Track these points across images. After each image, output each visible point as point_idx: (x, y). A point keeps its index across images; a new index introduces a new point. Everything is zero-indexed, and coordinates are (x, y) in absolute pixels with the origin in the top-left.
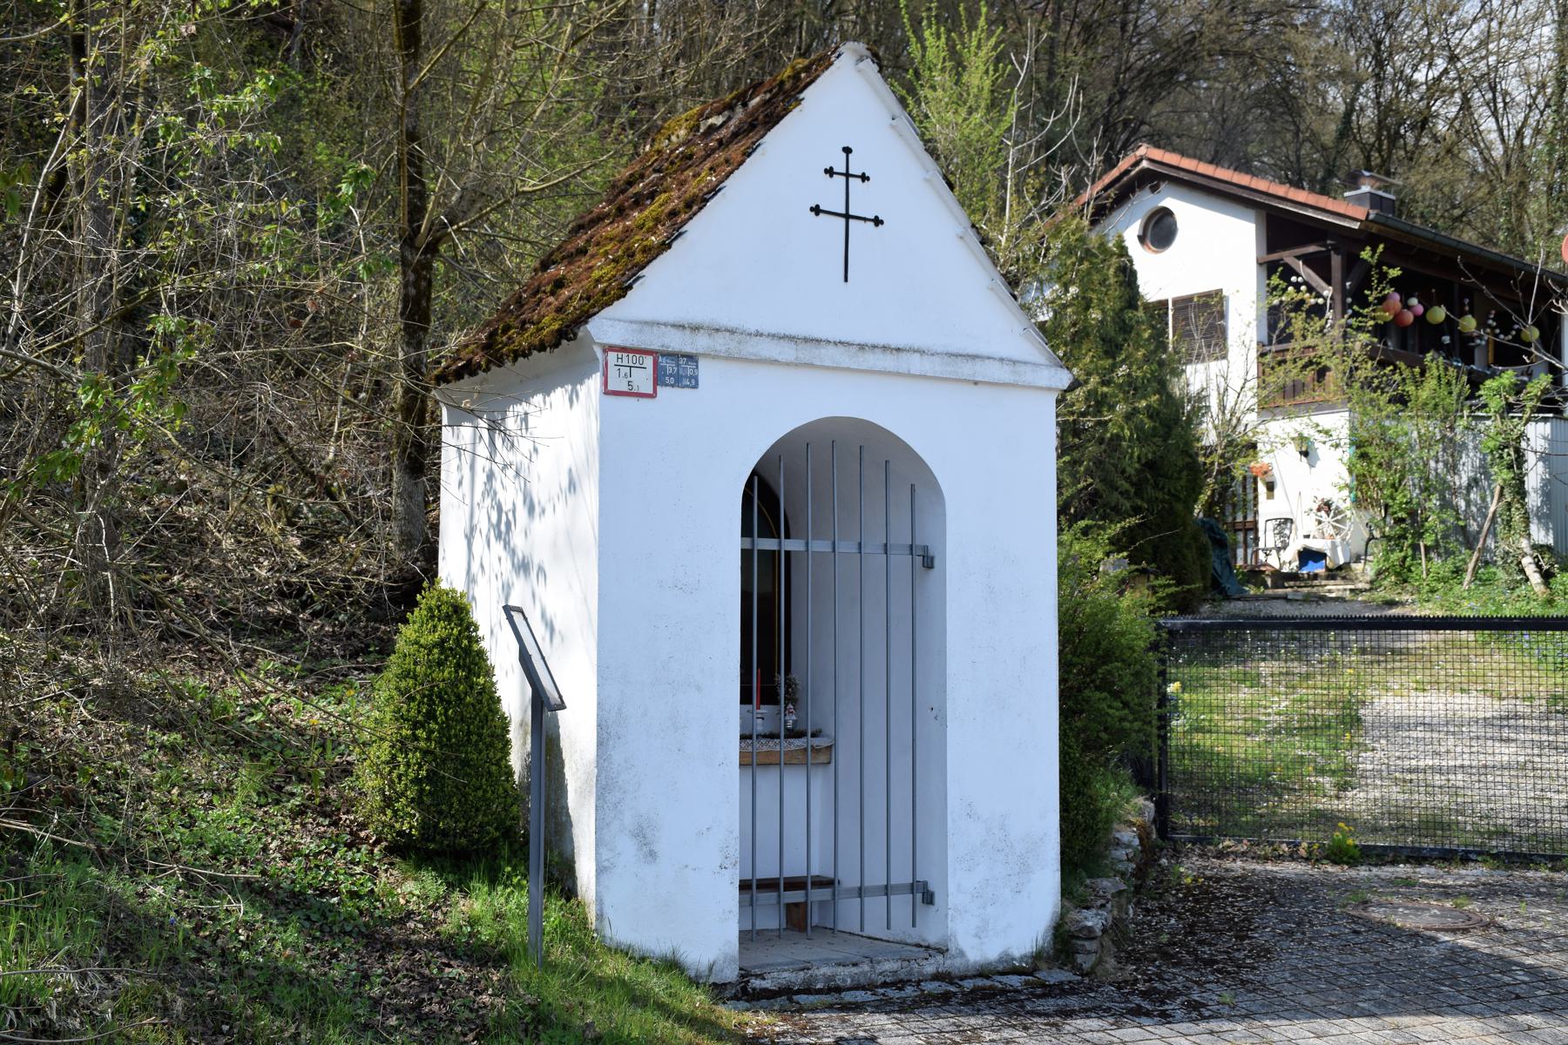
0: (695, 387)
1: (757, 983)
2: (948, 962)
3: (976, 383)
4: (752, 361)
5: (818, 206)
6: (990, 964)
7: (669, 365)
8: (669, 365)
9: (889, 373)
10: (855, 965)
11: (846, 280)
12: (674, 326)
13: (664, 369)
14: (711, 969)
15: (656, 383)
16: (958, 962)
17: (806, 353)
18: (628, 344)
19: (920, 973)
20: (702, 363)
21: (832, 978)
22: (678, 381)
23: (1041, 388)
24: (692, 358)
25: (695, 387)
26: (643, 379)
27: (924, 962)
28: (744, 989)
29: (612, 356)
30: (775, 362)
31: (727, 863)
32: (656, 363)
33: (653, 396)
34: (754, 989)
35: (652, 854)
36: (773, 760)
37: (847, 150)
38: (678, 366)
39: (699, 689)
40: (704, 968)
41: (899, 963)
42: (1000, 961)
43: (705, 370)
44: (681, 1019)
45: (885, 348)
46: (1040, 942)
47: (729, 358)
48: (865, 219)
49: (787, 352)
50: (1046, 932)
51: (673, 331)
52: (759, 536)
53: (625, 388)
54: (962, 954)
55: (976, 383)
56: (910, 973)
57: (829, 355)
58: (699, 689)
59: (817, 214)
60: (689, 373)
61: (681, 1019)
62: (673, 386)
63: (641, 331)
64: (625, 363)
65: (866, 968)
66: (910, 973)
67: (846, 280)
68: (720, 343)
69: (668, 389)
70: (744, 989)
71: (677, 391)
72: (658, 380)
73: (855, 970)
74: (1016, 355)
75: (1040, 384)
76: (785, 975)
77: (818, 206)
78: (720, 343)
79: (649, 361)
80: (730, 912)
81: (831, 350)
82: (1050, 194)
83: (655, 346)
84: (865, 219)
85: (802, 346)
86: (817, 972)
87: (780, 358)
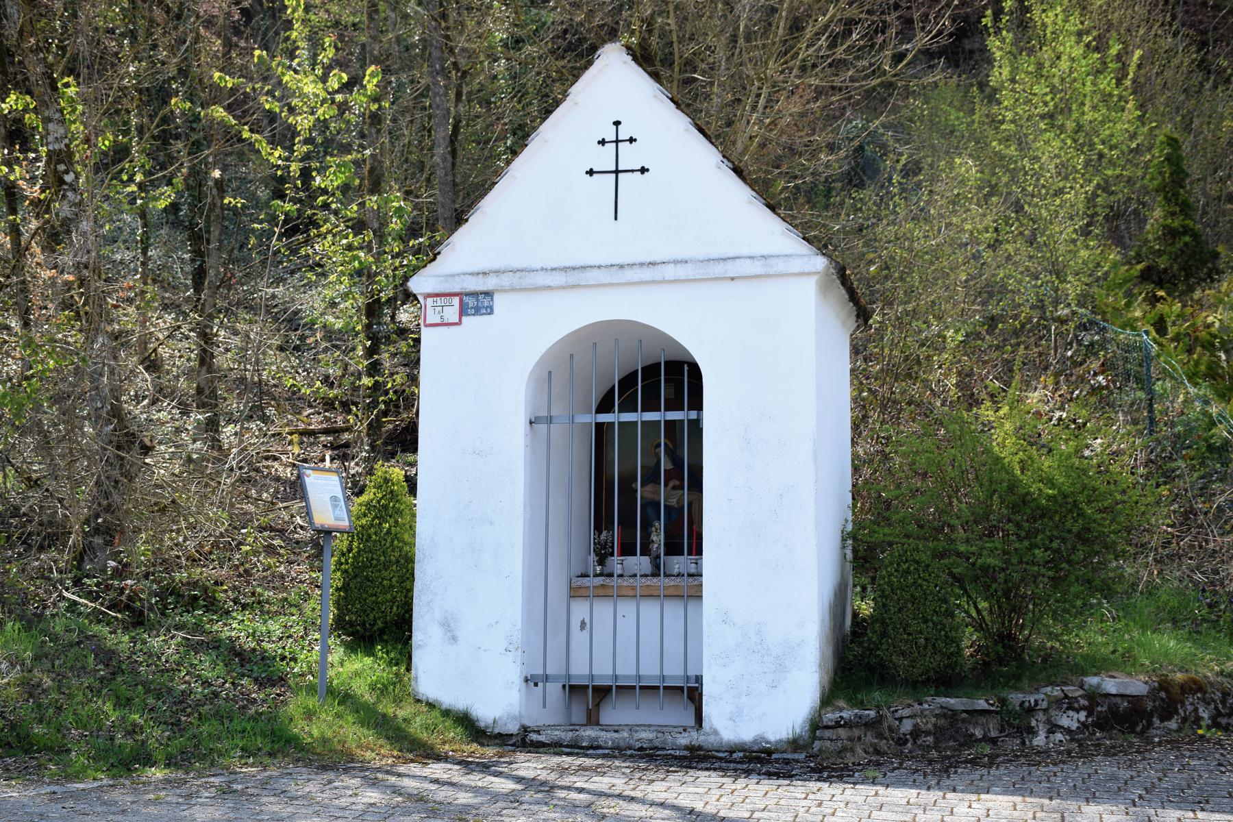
0: (491, 313)
1: (534, 737)
2: (702, 738)
3: (733, 279)
4: (530, 290)
5: (591, 169)
6: (745, 743)
7: (471, 302)
8: (471, 302)
9: (695, 280)
10: (616, 731)
11: (616, 219)
12: (472, 274)
13: (468, 304)
14: (495, 721)
15: (461, 315)
16: (712, 738)
17: (574, 278)
18: (437, 291)
19: (673, 744)
20: (496, 297)
21: (596, 739)
22: (477, 311)
23: (716, 279)
24: (488, 294)
25: (491, 313)
26: (452, 313)
27: (678, 735)
28: (523, 740)
29: (430, 301)
30: (550, 288)
31: (511, 648)
32: (461, 301)
33: (459, 323)
34: (532, 741)
35: (454, 639)
36: (680, 593)
37: (617, 123)
38: (478, 300)
39: (491, 523)
40: (490, 721)
41: (655, 734)
42: (755, 742)
43: (499, 301)
44: (652, 804)
45: (642, 264)
46: (798, 731)
47: (513, 290)
48: (632, 171)
49: (559, 279)
50: (804, 722)
51: (470, 277)
52: (614, 423)
53: (439, 321)
54: (716, 732)
55: (733, 279)
56: (664, 742)
57: (592, 277)
58: (491, 523)
59: (591, 175)
60: (486, 304)
61: (652, 804)
62: (474, 315)
63: (446, 281)
64: (439, 304)
65: (626, 735)
66: (664, 742)
67: (616, 219)
68: (505, 281)
69: (471, 318)
70: (523, 740)
71: (478, 318)
72: (463, 312)
73: (616, 735)
74: (789, 252)
75: (792, 271)
76: (557, 733)
77: (591, 169)
78: (505, 281)
79: (456, 300)
80: (513, 683)
81: (595, 272)
82: (404, 146)
83: (457, 290)
84: (632, 171)
85: (570, 273)
86: (583, 733)
87: (552, 285)
